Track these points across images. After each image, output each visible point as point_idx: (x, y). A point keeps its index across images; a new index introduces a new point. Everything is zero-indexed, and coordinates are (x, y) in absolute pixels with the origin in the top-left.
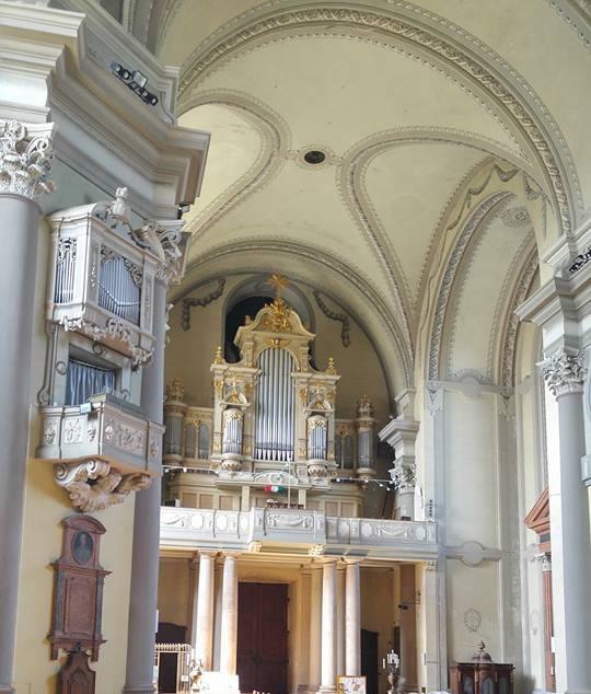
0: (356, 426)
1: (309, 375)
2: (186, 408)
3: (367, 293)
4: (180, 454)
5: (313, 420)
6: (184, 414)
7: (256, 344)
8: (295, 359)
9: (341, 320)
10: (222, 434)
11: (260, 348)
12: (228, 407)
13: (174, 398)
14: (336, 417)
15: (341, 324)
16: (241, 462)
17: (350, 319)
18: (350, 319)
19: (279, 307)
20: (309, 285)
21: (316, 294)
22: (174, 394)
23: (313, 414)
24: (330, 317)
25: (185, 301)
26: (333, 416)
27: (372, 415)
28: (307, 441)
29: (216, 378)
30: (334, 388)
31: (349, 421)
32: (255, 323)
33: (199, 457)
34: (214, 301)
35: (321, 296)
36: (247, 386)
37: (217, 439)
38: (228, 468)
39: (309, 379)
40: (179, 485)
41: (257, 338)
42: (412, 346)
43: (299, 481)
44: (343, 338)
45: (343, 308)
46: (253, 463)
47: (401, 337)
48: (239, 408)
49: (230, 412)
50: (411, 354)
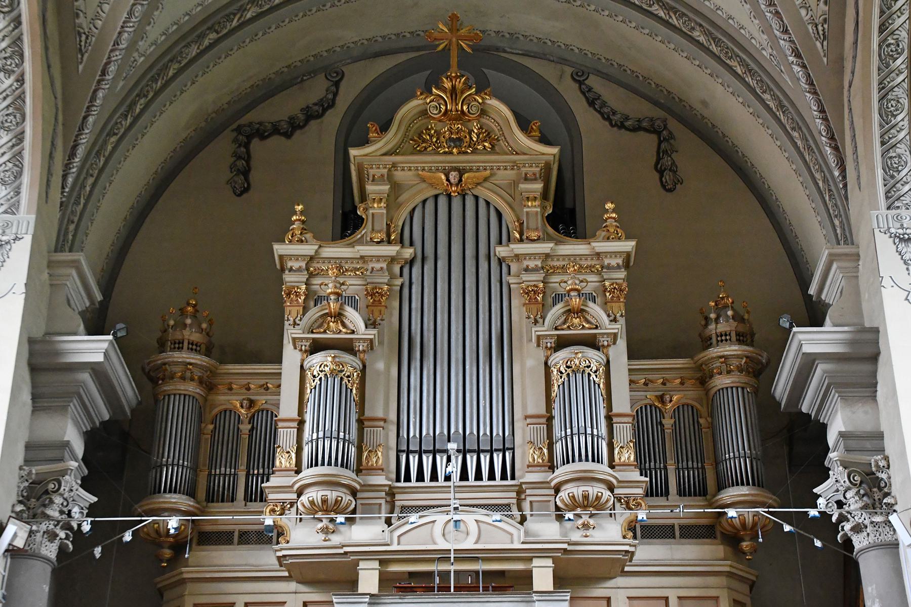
0: (703, 378)
1: (545, 247)
2: (213, 373)
3: (696, 34)
4: (191, 493)
5: (560, 358)
6: (209, 384)
7: (396, 188)
8: (509, 216)
9: (652, 130)
10: (301, 423)
11: (410, 199)
12: (316, 347)
13: (178, 345)
14: (632, 355)
15: (654, 137)
16: (354, 493)
17: (673, 125)
18: (673, 125)
19: (453, 92)
20: (563, 61)
21: (579, 78)
22: (178, 336)
23: (562, 343)
24: (621, 126)
25: (238, 130)
26: (622, 344)
27: (742, 338)
28: (550, 419)
29: (288, 278)
30: (622, 274)
31: (679, 363)
32: (391, 138)
33: (248, 498)
34: (313, 124)
35: (593, 82)
36: (374, 294)
37: (286, 437)
38: (313, 508)
39: (547, 256)
40: (183, 582)
41: (399, 175)
42: (832, 138)
43: (527, 533)
44: (661, 173)
45: (656, 103)
46: (391, 493)
47: (801, 124)
48: (347, 347)
49: (320, 361)
50: (832, 160)
